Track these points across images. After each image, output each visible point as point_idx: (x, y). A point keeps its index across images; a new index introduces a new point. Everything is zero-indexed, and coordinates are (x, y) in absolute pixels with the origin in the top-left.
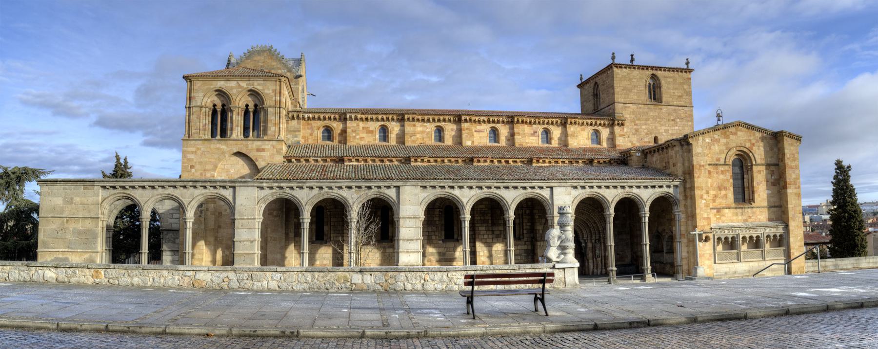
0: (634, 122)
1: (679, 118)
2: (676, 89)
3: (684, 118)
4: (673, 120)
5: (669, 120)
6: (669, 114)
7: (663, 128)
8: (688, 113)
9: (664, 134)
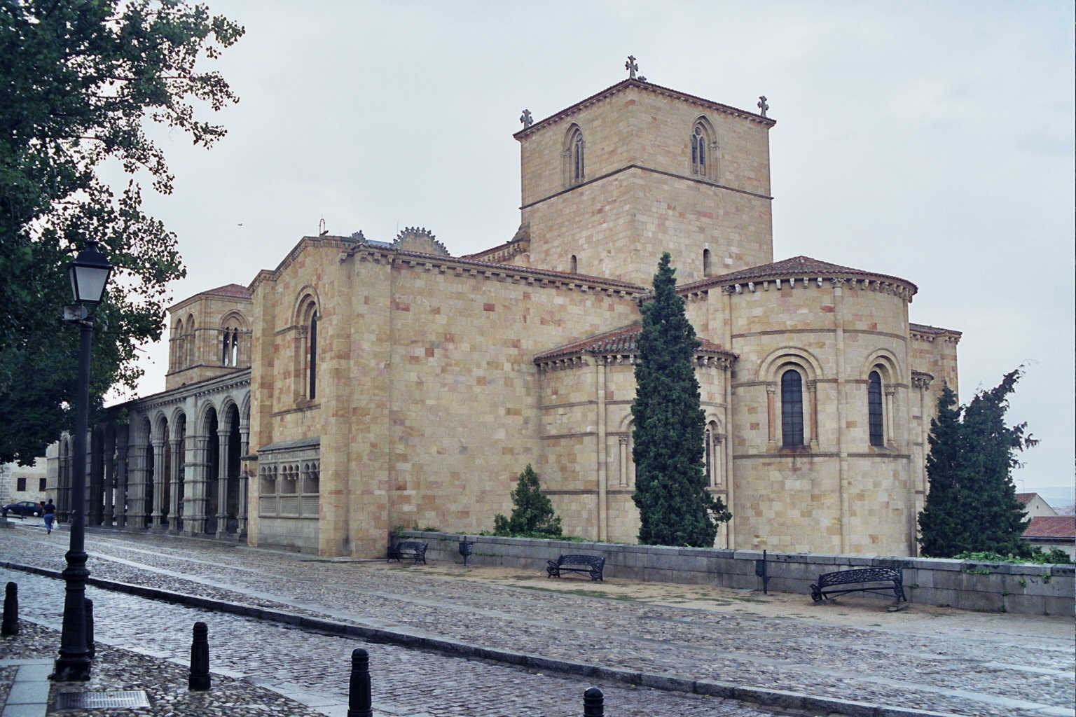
0: (544, 236)
1: (609, 203)
2: (606, 138)
3: (618, 197)
4: (600, 211)
5: (593, 214)
6: (593, 199)
7: (585, 233)
8: (625, 184)
9: (586, 246)
